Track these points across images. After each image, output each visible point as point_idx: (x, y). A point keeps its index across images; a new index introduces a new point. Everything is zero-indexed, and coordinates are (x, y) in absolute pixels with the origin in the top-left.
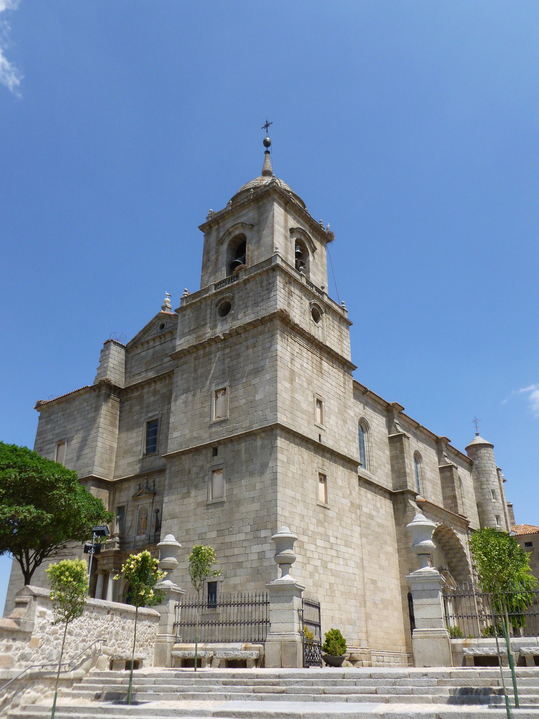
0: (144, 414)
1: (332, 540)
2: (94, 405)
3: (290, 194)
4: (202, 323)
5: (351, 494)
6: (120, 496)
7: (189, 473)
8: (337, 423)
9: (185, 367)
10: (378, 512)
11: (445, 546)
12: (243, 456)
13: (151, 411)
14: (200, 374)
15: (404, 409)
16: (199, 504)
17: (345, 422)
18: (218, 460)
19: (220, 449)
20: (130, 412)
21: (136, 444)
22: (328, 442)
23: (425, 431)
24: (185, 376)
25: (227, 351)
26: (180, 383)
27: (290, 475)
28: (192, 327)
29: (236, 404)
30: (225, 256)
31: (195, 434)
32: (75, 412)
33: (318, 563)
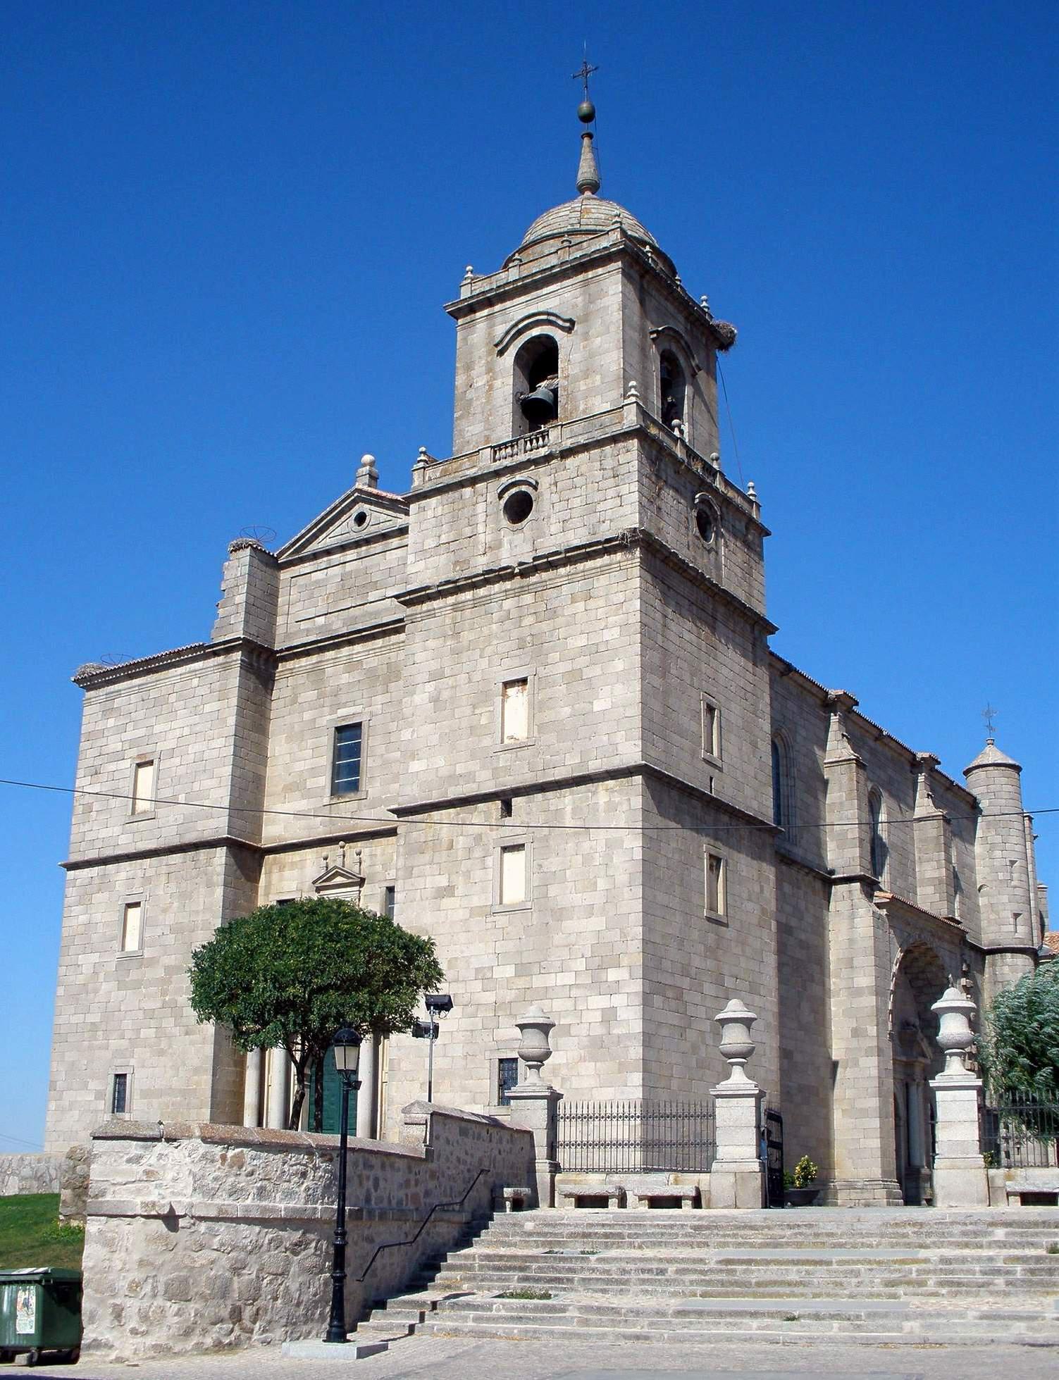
1: (729, 982)
2: (216, 686)
3: (648, 248)
4: (468, 531)
5: (762, 891)
6: (281, 880)
7: (451, 847)
9: (431, 622)
10: (801, 919)
11: (917, 978)
13: (345, 705)
14: (465, 643)
15: (857, 704)
17: (754, 745)
19: (517, 802)
20: (294, 701)
21: (314, 772)
22: (723, 790)
23: (892, 744)
25: (528, 598)
26: (418, 658)
27: (662, 862)
28: (444, 539)
29: (548, 716)
31: (460, 769)
32: (173, 698)
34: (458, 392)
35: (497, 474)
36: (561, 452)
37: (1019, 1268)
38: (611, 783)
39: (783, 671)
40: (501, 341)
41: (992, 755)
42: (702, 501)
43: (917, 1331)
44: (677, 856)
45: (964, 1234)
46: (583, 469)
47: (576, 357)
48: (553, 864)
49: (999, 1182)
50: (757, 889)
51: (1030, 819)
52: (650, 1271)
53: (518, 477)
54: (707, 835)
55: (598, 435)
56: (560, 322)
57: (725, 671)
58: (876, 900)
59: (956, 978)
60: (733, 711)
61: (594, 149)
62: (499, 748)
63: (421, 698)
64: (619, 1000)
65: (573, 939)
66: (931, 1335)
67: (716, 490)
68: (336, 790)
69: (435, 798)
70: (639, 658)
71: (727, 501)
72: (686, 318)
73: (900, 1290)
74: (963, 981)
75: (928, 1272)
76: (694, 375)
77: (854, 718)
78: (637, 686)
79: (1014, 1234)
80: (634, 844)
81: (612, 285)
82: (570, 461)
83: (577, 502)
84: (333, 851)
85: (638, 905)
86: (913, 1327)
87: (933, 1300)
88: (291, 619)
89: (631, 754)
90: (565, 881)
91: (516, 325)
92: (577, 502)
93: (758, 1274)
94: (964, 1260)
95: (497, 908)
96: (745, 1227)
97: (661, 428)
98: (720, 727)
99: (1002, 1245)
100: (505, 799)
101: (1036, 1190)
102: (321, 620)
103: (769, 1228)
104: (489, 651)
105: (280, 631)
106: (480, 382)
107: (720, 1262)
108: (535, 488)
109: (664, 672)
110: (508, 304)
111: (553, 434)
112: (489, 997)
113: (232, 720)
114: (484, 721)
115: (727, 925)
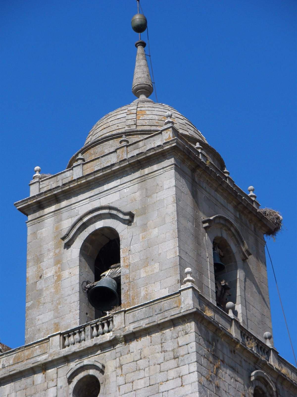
3: (198, 145)
30: (76, 271)
34: (29, 283)
35: (66, 359)
36: (125, 336)
40: (68, 235)
42: (258, 378)
46: (146, 352)
47: (136, 247)
53: (86, 361)
55: (158, 319)
56: (121, 216)
61: (147, 56)
67: (270, 368)
71: (281, 378)
72: (235, 207)
76: (245, 259)
81: (166, 180)
82: (134, 345)
83: (140, 384)
91: (81, 219)
92: (140, 384)
97: (215, 310)
106: (50, 273)
108: (102, 372)
110: (74, 200)
111: (118, 320)
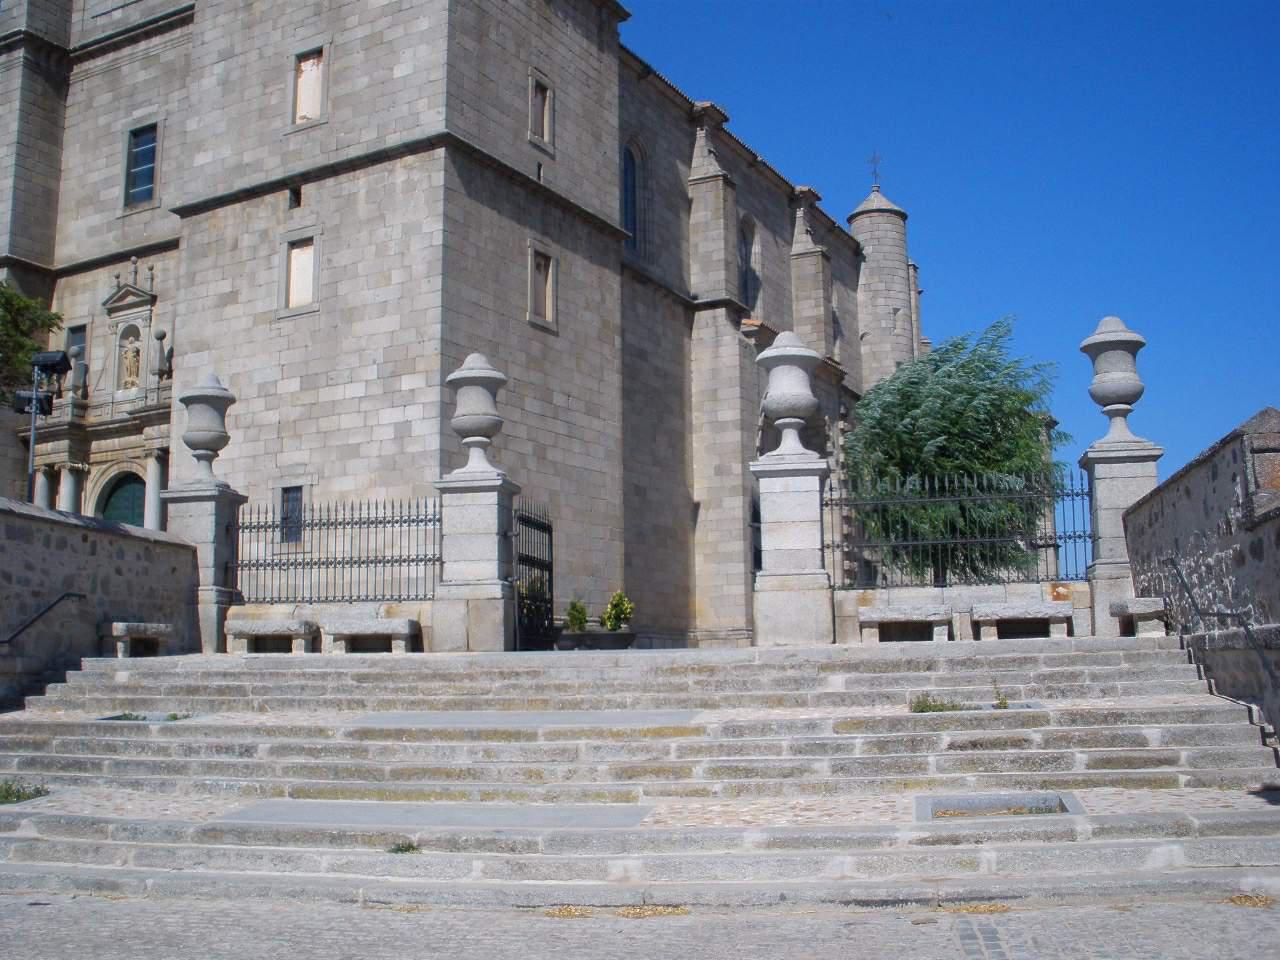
0: (122, 113)
1: (559, 399)
5: (603, 300)
7: (235, 247)
8: (578, 139)
12: (363, 209)
16: (257, 319)
17: (598, 138)
18: (302, 220)
20: (89, 106)
21: (108, 182)
24: (222, 19)
29: (344, 89)
31: (247, 158)
33: (528, 448)
37: (859, 739)
38: (410, 159)
39: (637, 74)
41: (877, 201)
43: (636, 878)
44: (490, 247)
45: (779, 683)
48: (343, 258)
49: (849, 608)
50: (598, 298)
51: (915, 268)
52: (229, 749)
54: (532, 227)
57: (562, 50)
58: (744, 328)
59: (833, 420)
60: (571, 97)
62: (289, 129)
63: (209, 82)
64: (413, 412)
65: (363, 343)
66: (664, 886)
68: (131, 201)
69: (221, 191)
70: (446, 13)
73: (639, 786)
74: (841, 424)
75: (699, 751)
77: (725, 138)
78: (443, 44)
79: (858, 682)
80: (433, 229)
84: (125, 269)
85: (436, 299)
86: (628, 866)
87: (695, 804)
88: (87, 16)
89: (433, 121)
90: (356, 276)
93: (408, 755)
94: (764, 728)
95: (283, 313)
96: (434, 676)
98: (553, 110)
99: (839, 699)
100: (293, 186)
101: (902, 617)
102: (117, 15)
103: (471, 677)
104: (282, 22)
105: (76, 29)
107: (350, 734)
109: (481, 36)
112: (273, 417)
113: (14, 126)
114: (274, 101)
115: (556, 334)
